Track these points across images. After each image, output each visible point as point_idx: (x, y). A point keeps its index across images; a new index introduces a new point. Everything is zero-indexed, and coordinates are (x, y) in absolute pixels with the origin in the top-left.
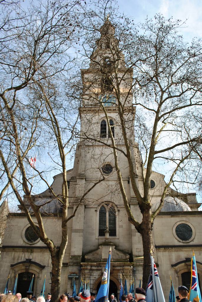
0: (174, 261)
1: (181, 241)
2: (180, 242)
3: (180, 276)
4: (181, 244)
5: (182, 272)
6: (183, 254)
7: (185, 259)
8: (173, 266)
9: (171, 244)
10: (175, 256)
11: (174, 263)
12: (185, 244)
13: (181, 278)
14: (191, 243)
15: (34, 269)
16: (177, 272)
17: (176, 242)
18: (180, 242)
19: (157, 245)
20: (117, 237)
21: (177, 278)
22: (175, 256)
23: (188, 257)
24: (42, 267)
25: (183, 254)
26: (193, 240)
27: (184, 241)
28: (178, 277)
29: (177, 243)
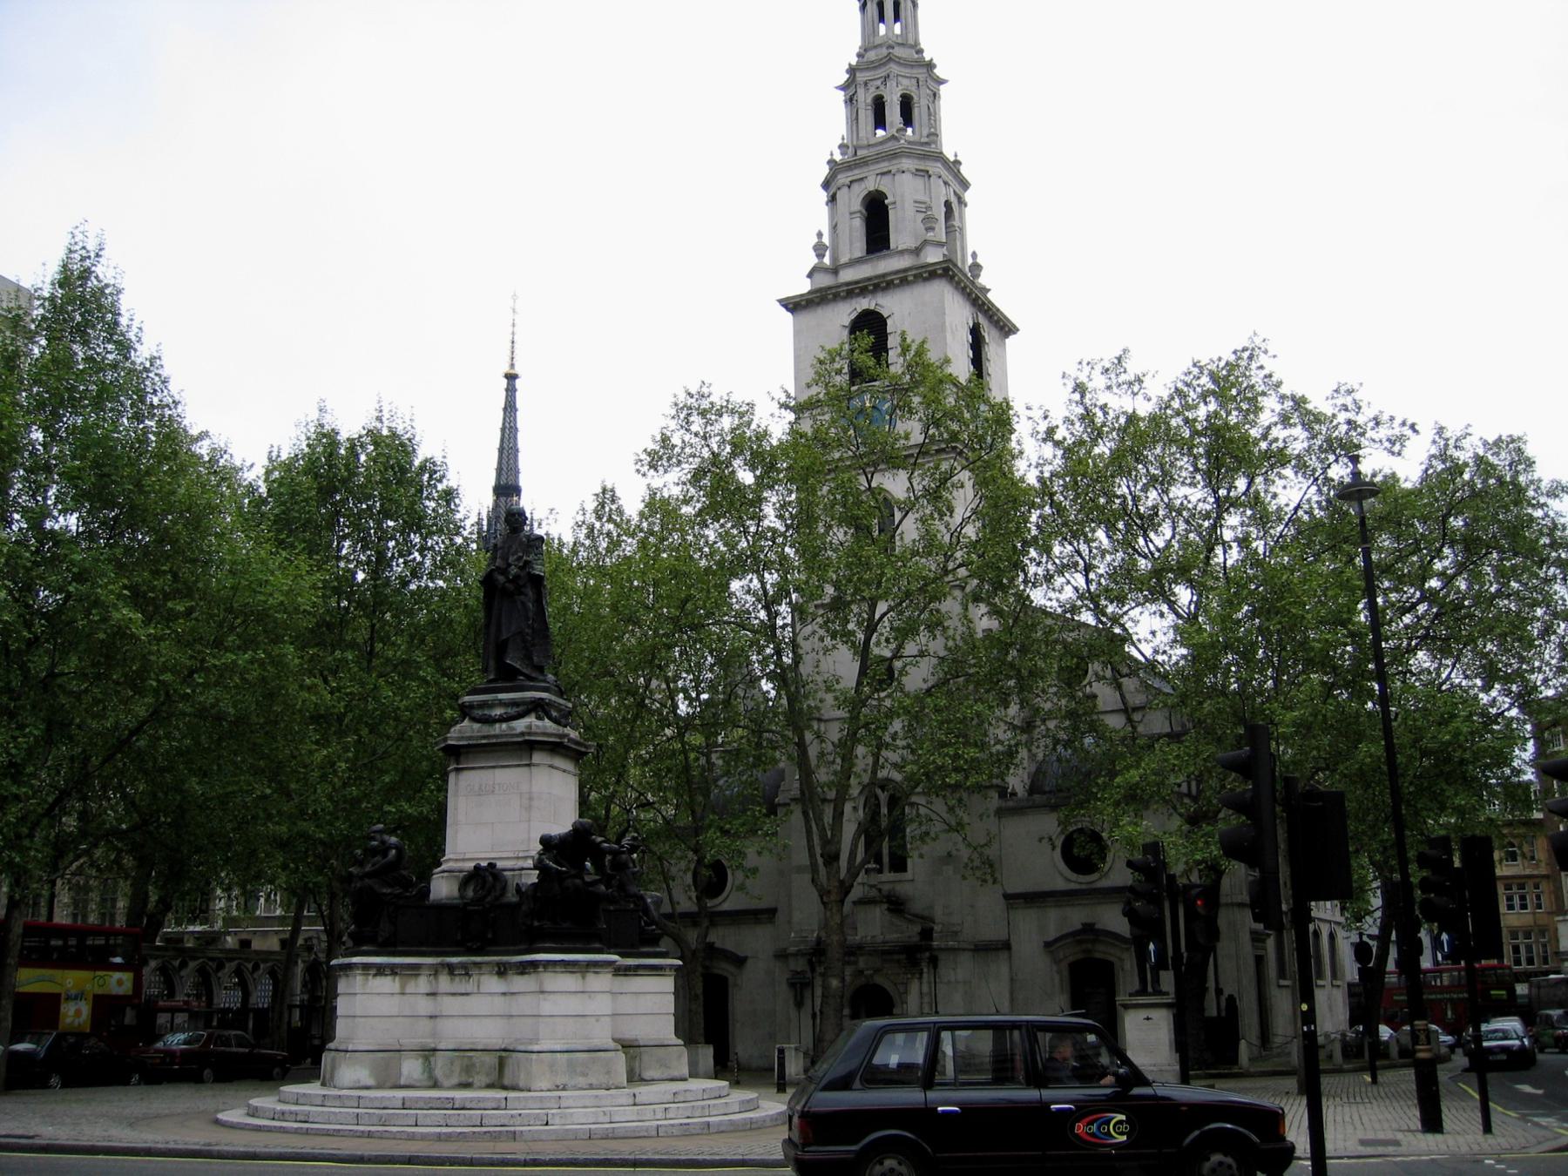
0: (1052, 934)
1: (1073, 876)
3: (1064, 966)
4: (1077, 887)
5: (1071, 959)
7: (1079, 927)
8: (1048, 945)
9: (1046, 888)
10: (1058, 921)
11: (1051, 939)
13: (1066, 973)
15: (723, 968)
16: (1057, 962)
17: (1059, 877)
19: (1010, 891)
20: (909, 875)
22: (1058, 921)
23: (1089, 921)
24: (740, 961)
25: (1076, 917)
28: (1059, 972)
29: (1060, 885)
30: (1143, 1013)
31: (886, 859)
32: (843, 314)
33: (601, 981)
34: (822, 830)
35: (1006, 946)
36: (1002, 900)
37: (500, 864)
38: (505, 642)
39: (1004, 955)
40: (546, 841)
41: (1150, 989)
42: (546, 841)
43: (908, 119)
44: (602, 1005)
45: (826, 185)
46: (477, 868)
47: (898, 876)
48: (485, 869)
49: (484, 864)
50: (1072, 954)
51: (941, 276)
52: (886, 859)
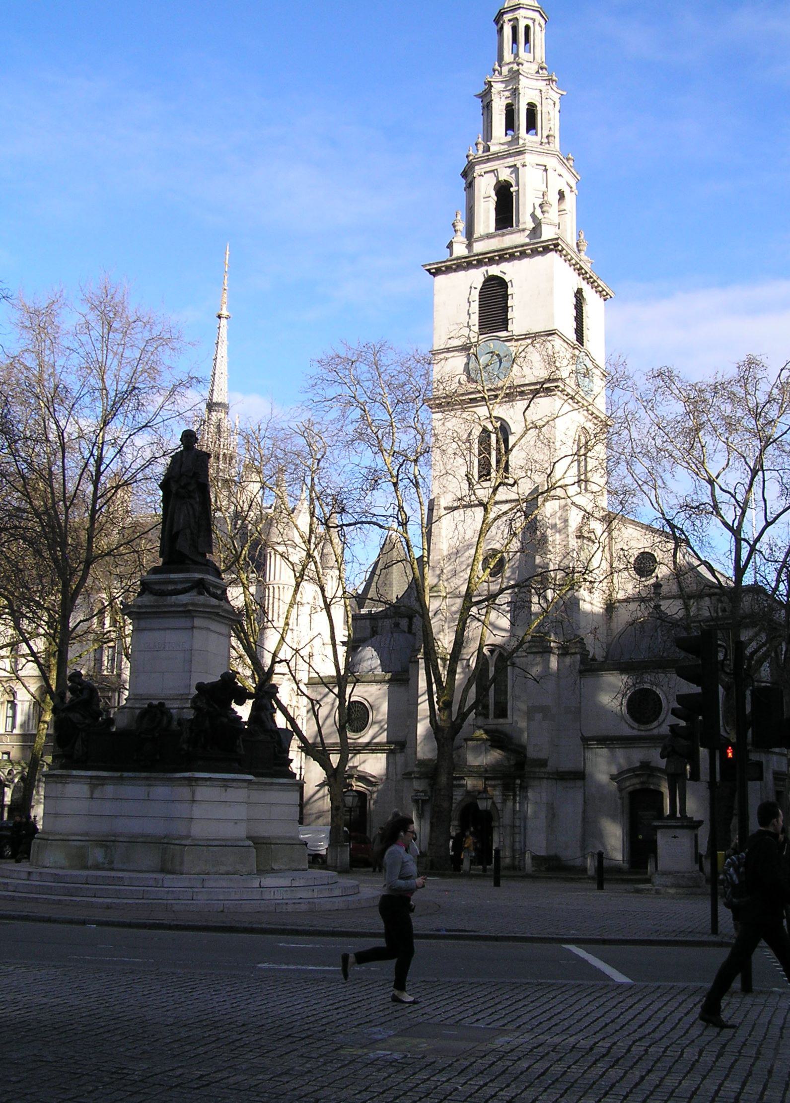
1: (636, 725)
2: (633, 728)
4: (635, 733)
5: (631, 789)
6: (638, 755)
7: (638, 764)
12: (643, 733)
14: (655, 732)
16: (620, 790)
18: (633, 728)
19: (587, 734)
21: (619, 801)
25: (638, 755)
26: (660, 725)
27: (642, 727)
29: (626, 731)
30: (672, 832)
31: (492, 707)
32: (477, 277)
33: (238, 794)
34: (439, 682)
35: (579, 776)
36: (579, 742)
37: (169, 704)
38: (177, 533)
39: (579, 783)
40: (200, 686)
41: (678, 815)
42: (200, 686)
43: (531, 125)
44: (240, 812)
45: (465, 174)
46: (150, 705)
47: (501, 721)
48: (156, 706)
49: (155, 702)
50: (633, 783)
51: (552, 250)
52: (492, 707)
